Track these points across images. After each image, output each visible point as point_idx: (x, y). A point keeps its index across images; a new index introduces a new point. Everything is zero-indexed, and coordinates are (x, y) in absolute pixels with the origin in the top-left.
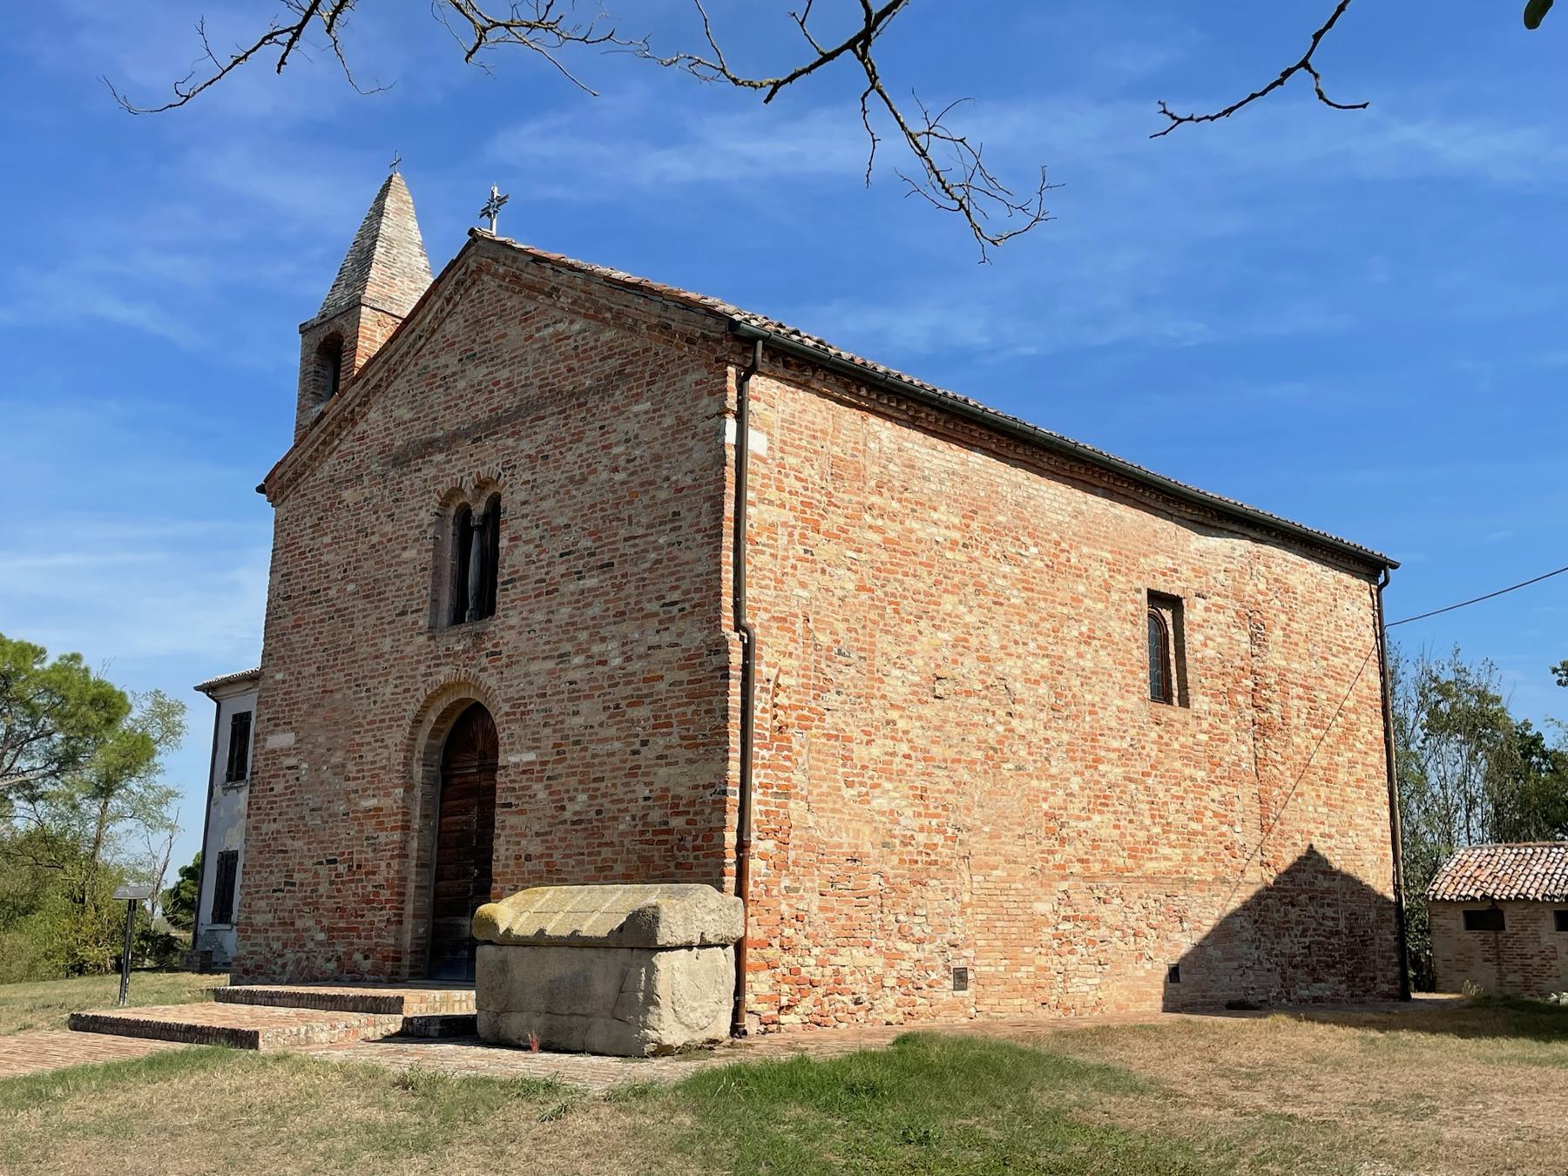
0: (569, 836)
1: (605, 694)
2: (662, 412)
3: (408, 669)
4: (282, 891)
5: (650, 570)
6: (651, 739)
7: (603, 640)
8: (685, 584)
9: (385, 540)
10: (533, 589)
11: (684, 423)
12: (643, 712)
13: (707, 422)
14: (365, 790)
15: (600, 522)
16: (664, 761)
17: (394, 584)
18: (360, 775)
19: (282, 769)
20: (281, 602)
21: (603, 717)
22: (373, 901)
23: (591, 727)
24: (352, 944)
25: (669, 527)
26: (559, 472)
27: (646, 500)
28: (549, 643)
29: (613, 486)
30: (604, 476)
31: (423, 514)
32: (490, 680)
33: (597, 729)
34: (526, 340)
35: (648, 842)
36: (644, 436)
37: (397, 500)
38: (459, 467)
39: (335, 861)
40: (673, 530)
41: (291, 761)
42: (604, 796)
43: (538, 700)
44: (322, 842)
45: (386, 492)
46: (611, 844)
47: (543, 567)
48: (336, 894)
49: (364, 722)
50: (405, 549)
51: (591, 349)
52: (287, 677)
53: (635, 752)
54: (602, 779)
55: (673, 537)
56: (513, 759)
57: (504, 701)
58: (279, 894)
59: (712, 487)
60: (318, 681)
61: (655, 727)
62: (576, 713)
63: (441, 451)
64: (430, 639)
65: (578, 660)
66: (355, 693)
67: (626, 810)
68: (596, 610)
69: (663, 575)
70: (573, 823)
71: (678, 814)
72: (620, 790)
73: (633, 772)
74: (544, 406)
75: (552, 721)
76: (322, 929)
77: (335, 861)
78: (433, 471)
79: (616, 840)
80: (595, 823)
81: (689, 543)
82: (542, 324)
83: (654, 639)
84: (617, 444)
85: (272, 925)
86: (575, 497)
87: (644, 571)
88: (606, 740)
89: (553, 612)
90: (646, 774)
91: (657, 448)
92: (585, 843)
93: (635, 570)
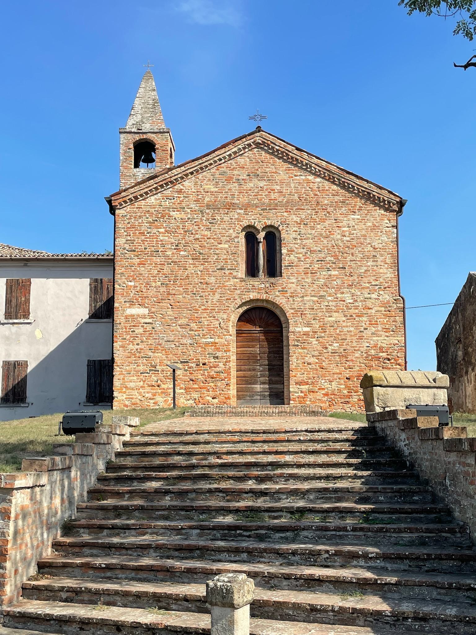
0: (330, 357)
1: (345, 311)
2: (366, 221)
3: (228, 291)
4: (147, 373)
5: (364, 273)
6: (369, 328)
7: (343, 293)
8: (381, 280)
9: (206, 238)
10: (303, 271)
11: (376, 227)
12: (365, 319)
13: (387, 229)
14: (204, 335)
15: (338, 253)
16: (375, 335)
17: (213, 256)
18: (201, 329)
19: (140, 323)
20: (127, 252)
21: (344, 319)
22: (216, 378)
23: (339, 322)
24: (204, 394)
25: (371, 260)
26: (314, 231)
27: (360, 249)
28: (314, 291)
29: (344, 241)
30: (339, 237)
31: (231, 231)
32: (280, 300)
33: (341, 323)
34: (289, 177)
35: (371, 360)
36: (356, 227)
37: (212, 223)
38: (253, 217)
39: (187, 362)
40: (373, 261)
41: (150, 321)
42: (347, 345)
43: (310, 310)
44: (178, 354)
45: (204, 218)
46: (352, 361)
47: (308, 263)
48: (188, 374)
49: (200, 309)
50: (221, 244)
51: (327, 190)
52: (137, 285)
53: (361, 332)
54: (346, 339)
55: (375, 263)
56: (298, 329)
57: (290, 309)
58: (147, 375)
59: (391, 250)
60: (162, 289)
61: (369, 324)
62: (331, 316)
63: (241, 209)
64: (241, 281)
65: (330, 298)
66: (191, 296)
67: (358, 350)
68: (339, 282)
69: (370, 275)
70: (332, 353)
71: (384, 352)
72: (355, 344)
73: (361, 338)
74: (302, 205)
75: (318, 318)
76: (181, 388)
77: (187, 362)
78: (236, 216)
79: (354, 359)
80: (343, 353)
81: (382, 267)
82: (299, 174)
83: (367, 296)
84: (345, 227)
85: (141, 387)
86: (323, 241)
87: (362, 273)
88: (347, 326)
89: (315, 280)
90: (368, 339)
91: (364, 232)
92: (339, 360)
93: (358, 272)
